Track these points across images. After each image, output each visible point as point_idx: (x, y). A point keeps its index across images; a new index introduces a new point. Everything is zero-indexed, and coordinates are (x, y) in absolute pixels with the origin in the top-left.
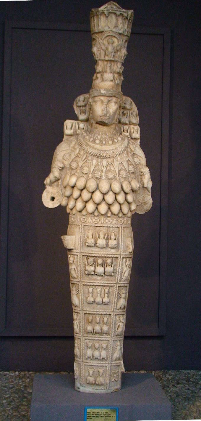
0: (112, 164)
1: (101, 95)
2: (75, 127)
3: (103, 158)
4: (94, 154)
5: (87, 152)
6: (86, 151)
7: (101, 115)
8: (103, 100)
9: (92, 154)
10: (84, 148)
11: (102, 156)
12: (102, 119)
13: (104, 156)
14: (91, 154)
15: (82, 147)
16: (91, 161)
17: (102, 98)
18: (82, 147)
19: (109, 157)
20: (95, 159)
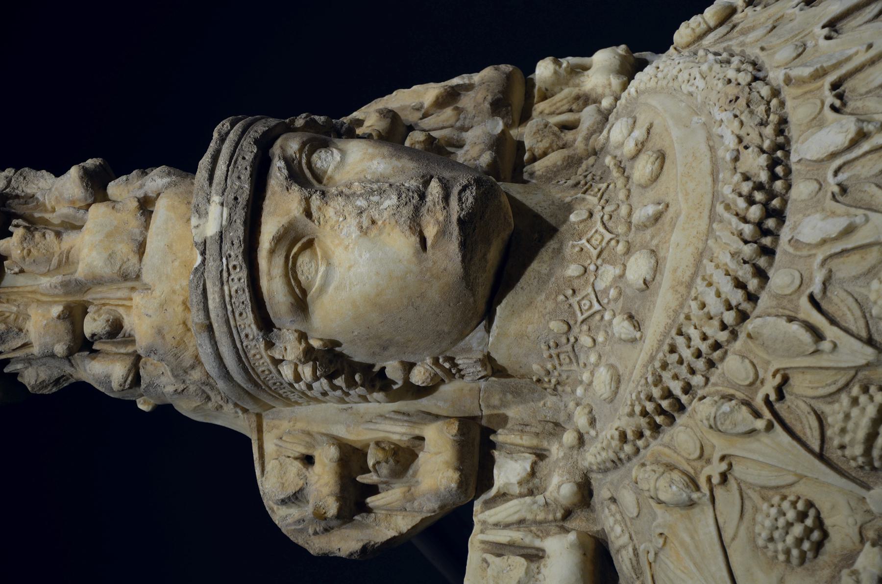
0: (835, 86)
1: (238, 232)
2: (521, 522)
3: (779, 170)
4: (748, 250)
5: (730, 317)
6: (723, 336)
7: (414, 240)
8: (284, 221)
9: (745, 273)
10: (700, 364)
11: (764, 177)
12: (443, 233)
13: (763, 160)
14: (753, 284)
15: (688, 389)
16: (820, 258)
17: (269, 229)
18: (688, 389)
19: (769, 131)
20: (794, 228)
